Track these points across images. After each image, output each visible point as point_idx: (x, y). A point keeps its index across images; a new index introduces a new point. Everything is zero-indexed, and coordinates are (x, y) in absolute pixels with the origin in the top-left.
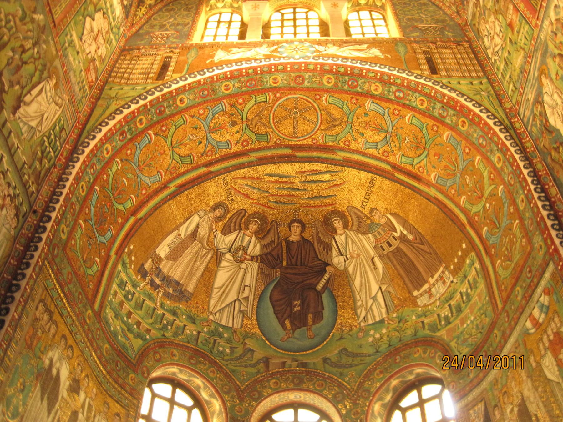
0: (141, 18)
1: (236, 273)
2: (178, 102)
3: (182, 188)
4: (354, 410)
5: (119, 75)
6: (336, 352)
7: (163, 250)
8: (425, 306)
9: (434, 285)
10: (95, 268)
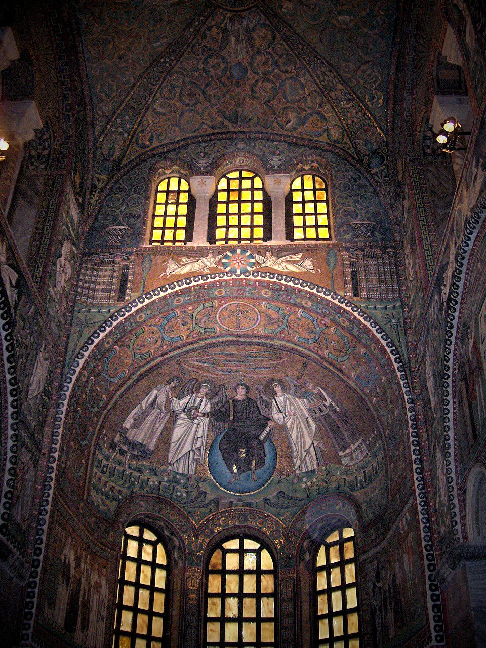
0: (94, 206)
1: (190, 429)
2: (138, 320)
3: (141, 377)
4: (287, 547)
5: (85, 291)
6: (275, 494)
7: (128, 423)
8: (347, 466)
9: (355, 452)
10: (82, 468)
